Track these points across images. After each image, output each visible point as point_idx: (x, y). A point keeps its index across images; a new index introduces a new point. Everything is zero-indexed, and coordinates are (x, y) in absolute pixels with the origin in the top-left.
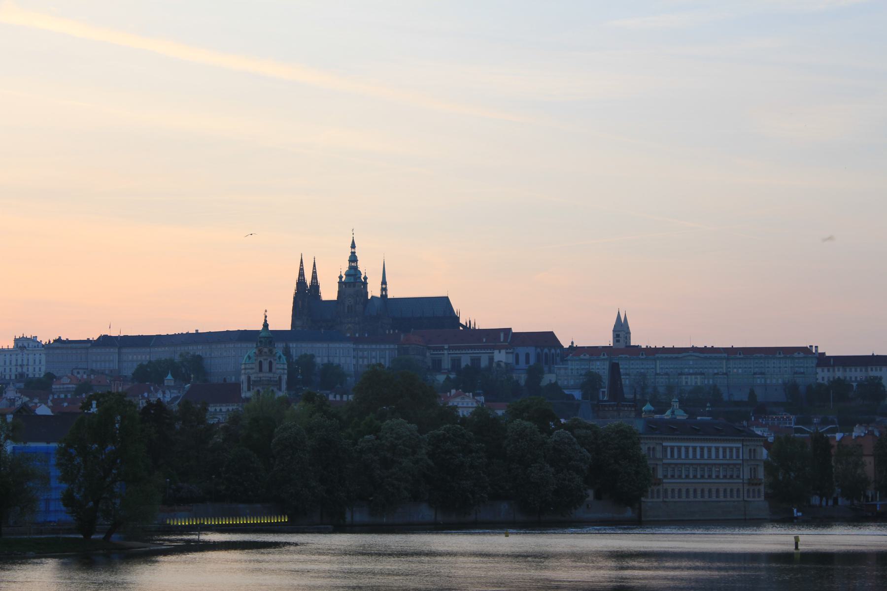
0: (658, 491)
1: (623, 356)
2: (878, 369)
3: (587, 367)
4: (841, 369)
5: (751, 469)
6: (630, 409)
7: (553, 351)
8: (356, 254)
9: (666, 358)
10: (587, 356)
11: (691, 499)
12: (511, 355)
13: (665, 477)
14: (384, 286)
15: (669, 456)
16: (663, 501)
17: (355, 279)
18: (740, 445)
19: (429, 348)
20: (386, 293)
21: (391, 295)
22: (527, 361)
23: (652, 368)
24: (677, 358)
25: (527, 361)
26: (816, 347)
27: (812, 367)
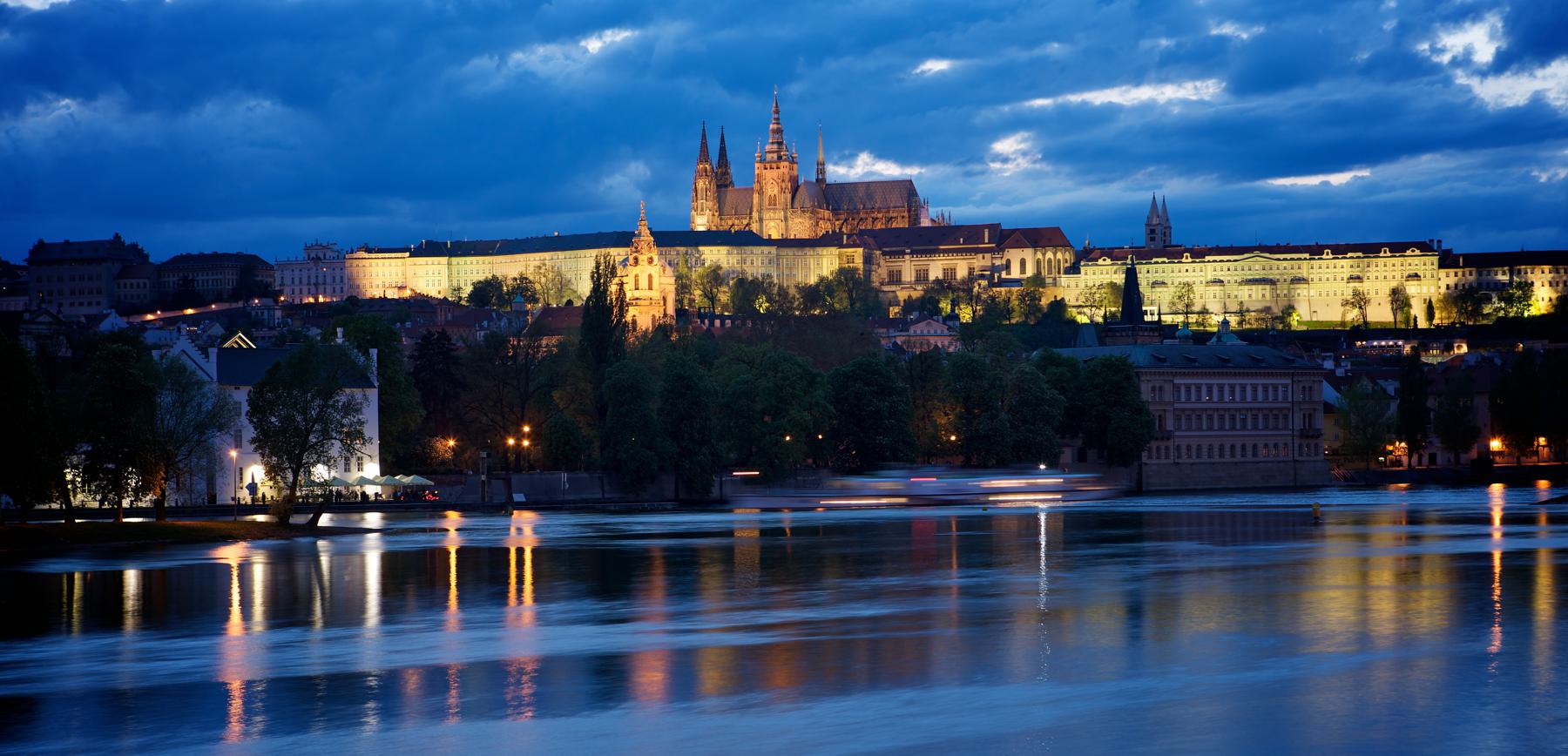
0: (1167, 448)
1: (1160, 260)
4: (1474, 273)
5: (1304, 415)
6: (1151, 334)
7: (1059, 256)
11: (1216, 459)
13: (1179, 429)
14: (820, 167)
15: (1183, 399)
16: (1175, 463)
17: (780, 158)
18: (1289, 381)
22: (1023, 270)
25: (1023, 270)
26: (1439, 241)
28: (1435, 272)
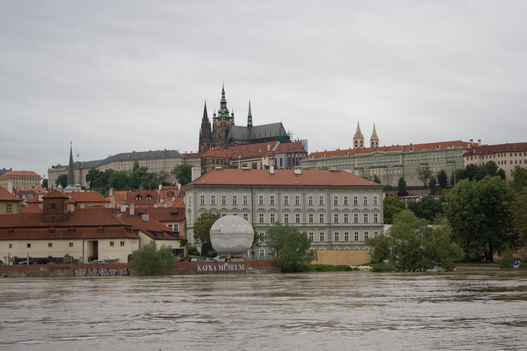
1: (335, 156)
2: (504, 155)
3: (313, 166)
4: (478, 157)
7: (297, 156)
8: (225, 98)
9: (361, 157)
10: (313, 159)
12: (272, 161)
17: (221, 115)
19: (231, 159)
20: (251, 123)
21: (254, 124)
23: (353, 164)
24: (368, 156)
27: (460, 157)
28: (462, 158)
